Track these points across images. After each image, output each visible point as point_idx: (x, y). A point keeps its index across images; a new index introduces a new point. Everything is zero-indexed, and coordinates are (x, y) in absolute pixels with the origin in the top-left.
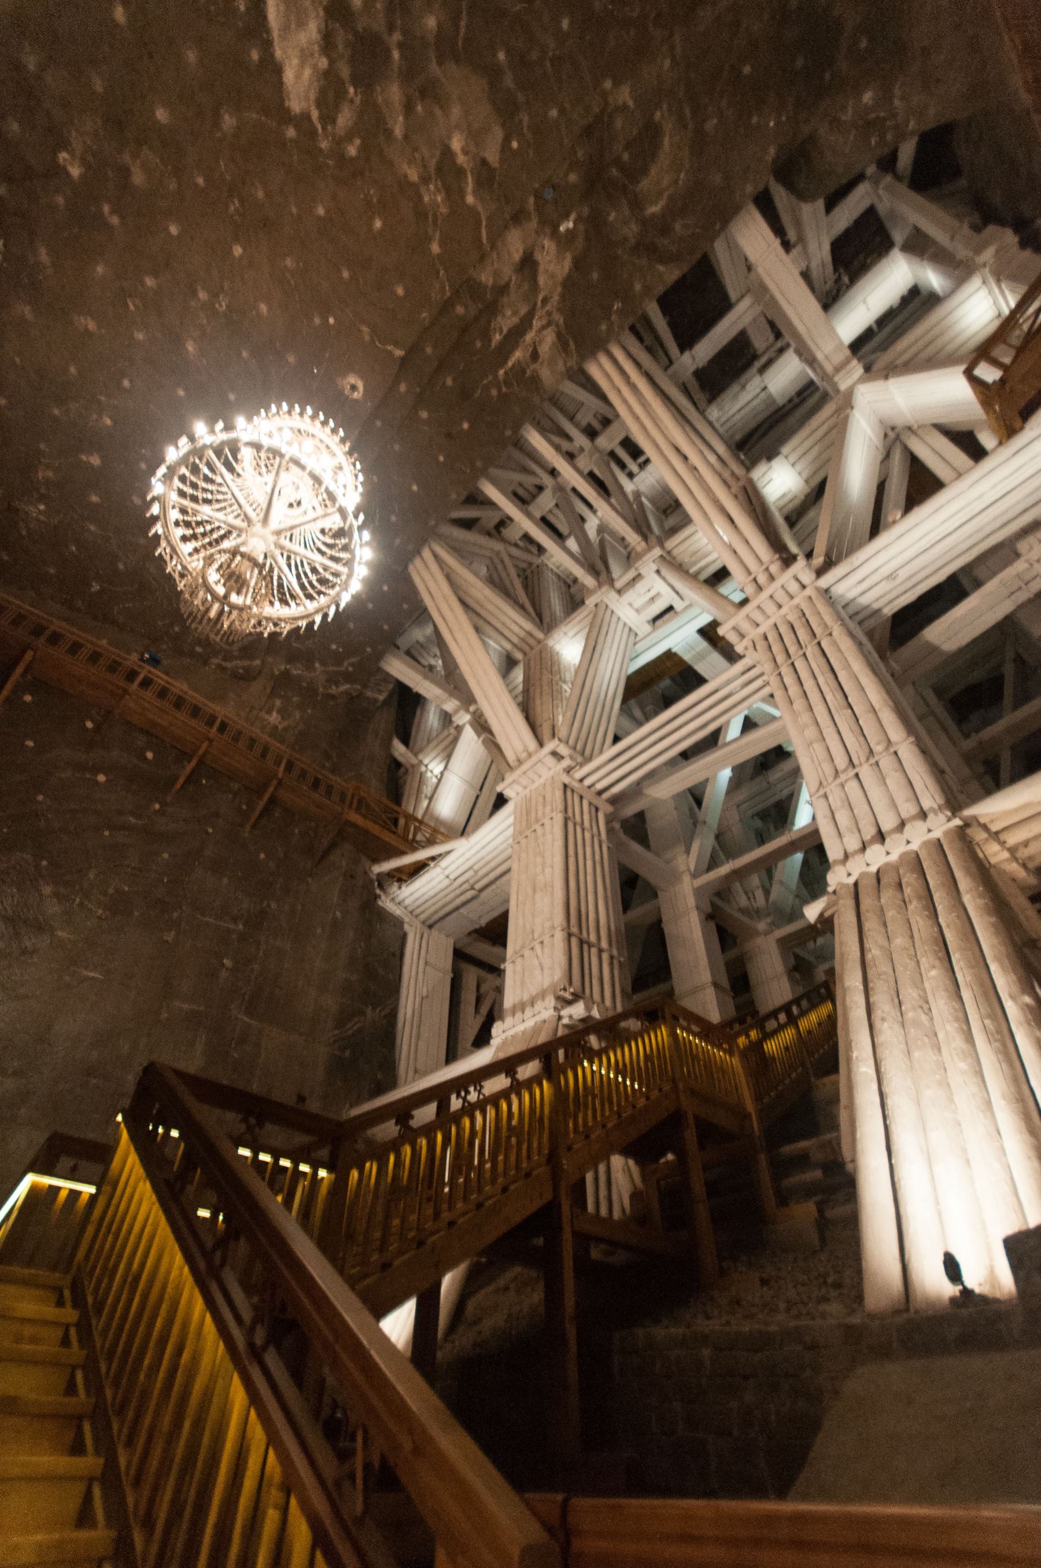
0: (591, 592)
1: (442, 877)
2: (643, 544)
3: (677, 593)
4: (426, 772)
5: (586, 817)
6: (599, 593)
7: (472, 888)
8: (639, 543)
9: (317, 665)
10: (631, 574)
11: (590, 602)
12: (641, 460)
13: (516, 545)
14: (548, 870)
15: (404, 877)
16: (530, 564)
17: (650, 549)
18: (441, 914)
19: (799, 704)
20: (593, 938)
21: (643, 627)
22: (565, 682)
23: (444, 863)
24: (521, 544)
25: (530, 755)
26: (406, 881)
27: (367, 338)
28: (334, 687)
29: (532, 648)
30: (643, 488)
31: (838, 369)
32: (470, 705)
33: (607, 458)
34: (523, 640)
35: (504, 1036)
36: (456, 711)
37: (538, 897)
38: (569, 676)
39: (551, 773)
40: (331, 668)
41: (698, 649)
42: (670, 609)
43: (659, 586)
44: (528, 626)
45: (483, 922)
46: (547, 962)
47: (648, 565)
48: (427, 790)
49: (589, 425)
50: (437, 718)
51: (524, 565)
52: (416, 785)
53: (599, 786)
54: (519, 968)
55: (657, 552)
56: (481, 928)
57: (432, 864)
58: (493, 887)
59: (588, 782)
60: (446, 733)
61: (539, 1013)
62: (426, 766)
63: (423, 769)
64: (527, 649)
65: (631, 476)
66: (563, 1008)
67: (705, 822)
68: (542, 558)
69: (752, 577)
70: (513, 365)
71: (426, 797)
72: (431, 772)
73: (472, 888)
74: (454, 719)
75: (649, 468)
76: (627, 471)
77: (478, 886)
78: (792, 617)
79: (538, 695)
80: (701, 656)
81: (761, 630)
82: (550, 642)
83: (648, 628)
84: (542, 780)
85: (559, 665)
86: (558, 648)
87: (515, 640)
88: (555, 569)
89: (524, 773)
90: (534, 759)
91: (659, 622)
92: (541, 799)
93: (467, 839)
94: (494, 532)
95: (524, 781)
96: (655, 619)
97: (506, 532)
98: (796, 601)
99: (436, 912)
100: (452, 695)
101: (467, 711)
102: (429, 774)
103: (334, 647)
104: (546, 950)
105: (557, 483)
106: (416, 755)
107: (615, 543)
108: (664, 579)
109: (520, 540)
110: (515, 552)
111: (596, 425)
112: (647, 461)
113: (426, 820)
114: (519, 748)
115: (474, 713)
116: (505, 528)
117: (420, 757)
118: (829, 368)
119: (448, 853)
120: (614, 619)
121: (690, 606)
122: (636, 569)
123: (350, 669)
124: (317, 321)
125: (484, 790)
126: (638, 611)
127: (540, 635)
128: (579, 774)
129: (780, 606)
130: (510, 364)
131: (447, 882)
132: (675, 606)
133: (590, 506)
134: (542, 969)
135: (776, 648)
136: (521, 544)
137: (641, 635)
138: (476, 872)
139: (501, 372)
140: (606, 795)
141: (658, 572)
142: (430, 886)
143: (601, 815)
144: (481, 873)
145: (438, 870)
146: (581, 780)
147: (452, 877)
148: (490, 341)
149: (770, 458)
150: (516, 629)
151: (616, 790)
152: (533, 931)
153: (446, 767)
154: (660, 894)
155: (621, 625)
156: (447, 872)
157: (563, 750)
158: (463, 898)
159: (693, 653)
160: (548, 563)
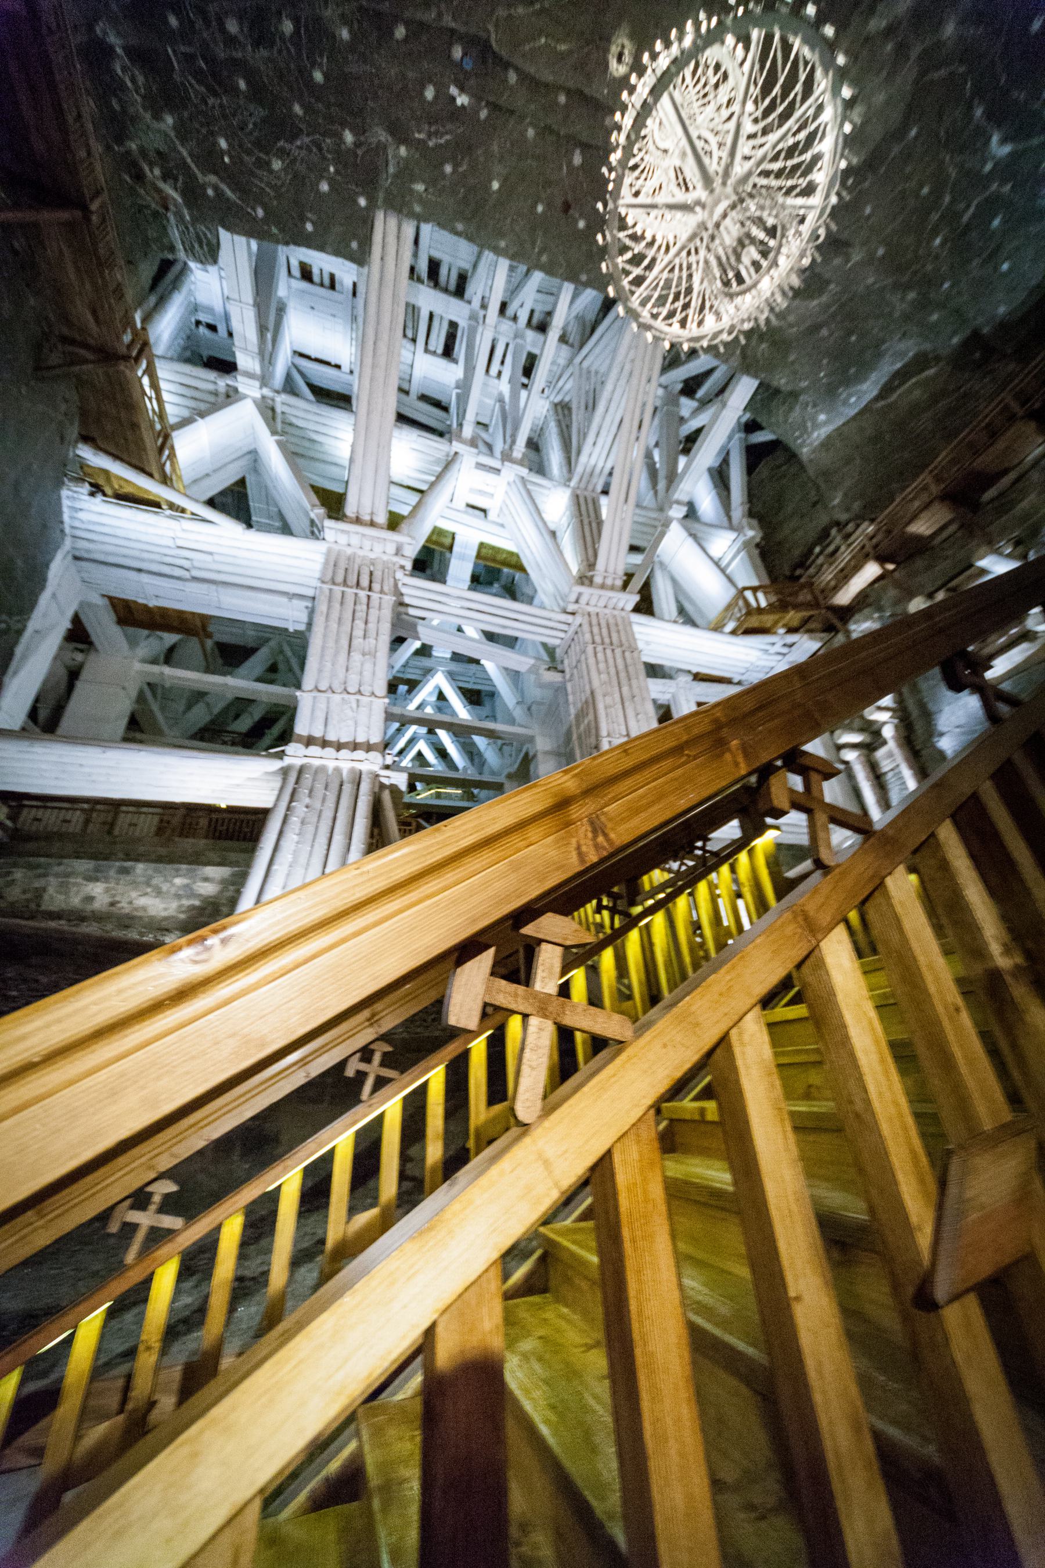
7: (187, 570)
9: (170, 120)
10: (496, 463)
11: (457, 446)
14: (372, 641)
15: (108, 491)
17: (520, 463)
18: (111, 559)
19: (604, 677)
25: (372, 524)
26: (105, 495)
28: (157, 172)
31: (678, 502)
35: (305, 761)
37: (356, 656)
39: (385, 558)
40: (185, 153)
42: (484, 511)
53: (407, 600)
54: (322, 706)
55: (524, 472)
57: (168, 512)
58: (213, 587)
73: (187, 570)
77: (195, 573)
78: (612, 621)
80: (462, 557)
81: (590, 609)
83: (462, 506)
84: (372, 556)
89: (363, 535)
91: (471, 510)
95: (355, 540)
96: (469, 506)
98: (616, 612)
99: (107, 554)
101: (261, 388)
103: (223, 144)
121: (502, 526)
123: (210, 192)
131: (171, 543)
135: (596, 630)
137: (454, 505)
144: (215, 567)
145: (173, 523)
147: (180, 543)
151: (412, 611)
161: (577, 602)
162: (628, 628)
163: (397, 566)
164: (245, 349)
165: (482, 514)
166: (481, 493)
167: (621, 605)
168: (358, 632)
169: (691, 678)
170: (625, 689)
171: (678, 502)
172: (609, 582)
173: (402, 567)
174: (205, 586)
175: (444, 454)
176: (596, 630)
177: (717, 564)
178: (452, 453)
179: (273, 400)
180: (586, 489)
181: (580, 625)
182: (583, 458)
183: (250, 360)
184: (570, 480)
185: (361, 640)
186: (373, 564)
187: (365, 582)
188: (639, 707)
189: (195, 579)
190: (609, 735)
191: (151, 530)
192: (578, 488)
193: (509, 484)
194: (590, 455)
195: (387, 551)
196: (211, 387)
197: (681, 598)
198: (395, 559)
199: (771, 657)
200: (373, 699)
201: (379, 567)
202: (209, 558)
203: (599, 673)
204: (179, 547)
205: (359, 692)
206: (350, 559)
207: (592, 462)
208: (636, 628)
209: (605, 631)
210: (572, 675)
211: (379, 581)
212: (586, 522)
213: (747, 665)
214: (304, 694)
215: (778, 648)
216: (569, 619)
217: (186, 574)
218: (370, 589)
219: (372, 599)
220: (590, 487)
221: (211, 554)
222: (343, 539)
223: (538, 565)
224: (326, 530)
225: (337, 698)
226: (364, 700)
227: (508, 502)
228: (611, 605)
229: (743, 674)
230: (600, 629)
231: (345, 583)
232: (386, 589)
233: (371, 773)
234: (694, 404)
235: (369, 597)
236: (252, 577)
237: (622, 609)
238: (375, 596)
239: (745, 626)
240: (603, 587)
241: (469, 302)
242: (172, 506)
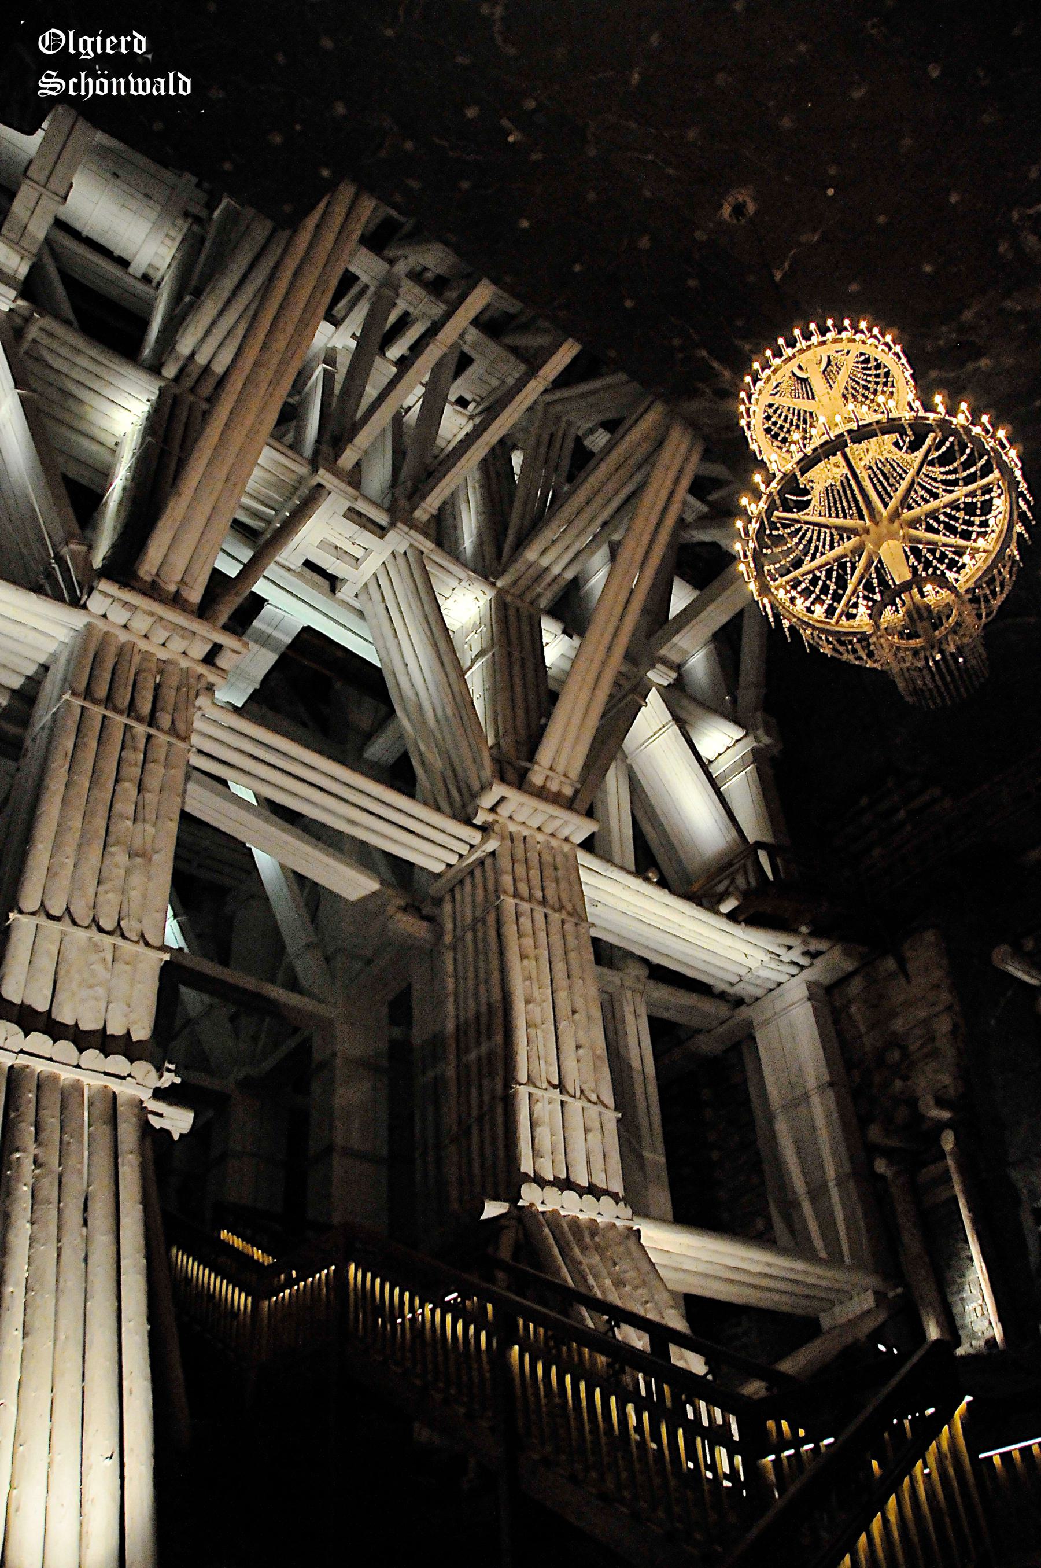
2: (425, 517)
6: (343, 486)
8: (425, 510)
10: (382, 519)
11: (324, 477)
17: (423, 530)
25: (176, 601)
27: (804, 239)
29: (192, 390)
31: (664, 661)
39: (184, 663)
41: (277, 634)
42: (333, 582)
47: (399, 540)
55: (427, 545)
69: (550, 773)
70: (714, 368)
78: (547, 858)
81: (512, 828)
83: (297, 563)
84: (162, 654)
91: (307, 572)
95: (141, 624)
96: (308, 564)
118: (663, 652)
121: (361, 614)
124: (832, 171)
129: (539, 829)
130: (715, 364)
139: (704, 353)
148: (744, 338)
149: (564, 632)
159: (269, 630)
161: (493, 809)
162: (573, 876)
165: (326, 584)
167: (565, 832)
168: (125, 807)
169: (647, 972)
170: (562, 995)
171: (664, 661)
172: (554, 787)
175: (295, 477)
176: (520, 869)
177: (704, 765)
180: (520, 597)
181: (493, 853)
182: (531, 554)
184: (497, 577)
185: (129, 823)
186: (161, 672)
187: (146, 708)
188: (581, 1033)
190: (530, 1081)
192: (507, 592)
193: (393, 553)
194: (544, 552)
195: (190, 653)
197: (640, 815)
198: (202, 669)
199: (782, 968)
200: (141, 948)
201: (174, 681)
203: (523, 956)
205: (119, 931)
206: (123, 652)
207: (545, 562)
208: (584, 876)
209: (535, 873)
210: (458, 940)
211: (170, 708)
212: (516, 655)
213: (743, 972)
215: (795, 955)
216: (476, 837)
218: (152, 721)
219: (154, 741)
220: (529, 596)
222: (118, 616)
223: (420, 707)
224: (95, 594)
227: (383, 581)
228: (549, 830)
229: (732, 984)
230: (528, 869)
231: (109, 701)
234: (705, 509)
235: (149, 737)
237: (566, 840)
238: (162, 738)
239: (752, 911)
240: (541, 794)
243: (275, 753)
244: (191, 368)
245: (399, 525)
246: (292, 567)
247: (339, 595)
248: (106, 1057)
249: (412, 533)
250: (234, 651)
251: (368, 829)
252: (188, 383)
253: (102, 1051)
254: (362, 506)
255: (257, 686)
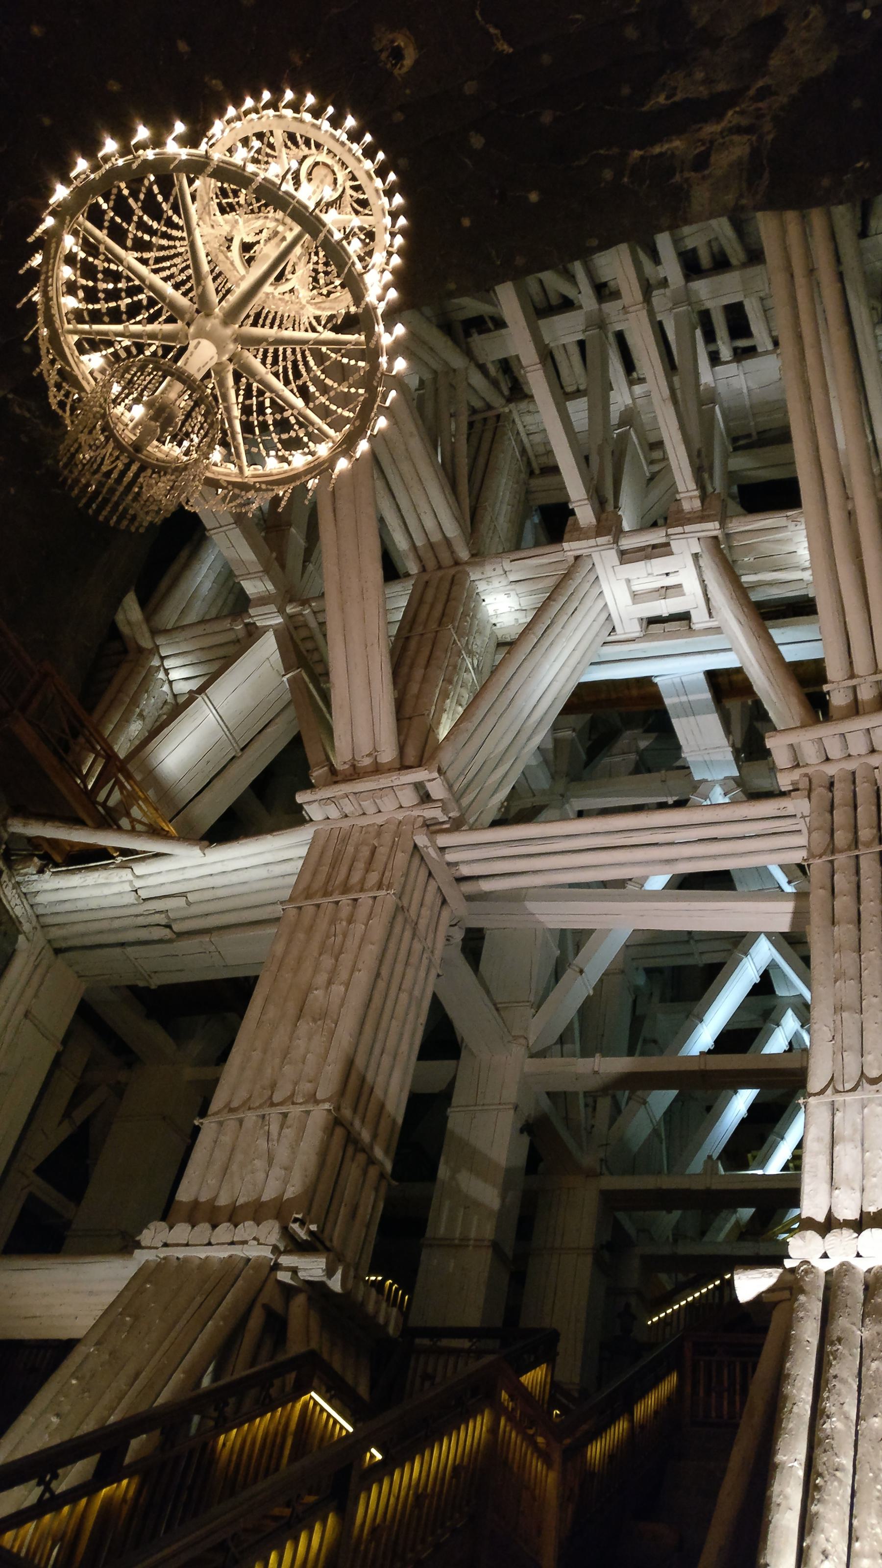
0: (582, 534)
1: (128, 888)
2: (697, 504)
3: (707, 600)
4: (158, 669)
5: (425, 912)
6: (592, 542)
7: (168, 926)
8: (691, 498)
11: (571, 548)
12: (742, 343)
13: (482, 368)
16: (489, 407)
17: (702, 517)
20: (366, 1136)
21: (630, 627)
22: (470, 653)
23: (140, 869)
24: (492, 370)
25: (377, 769)
30: (722, 389)
32: (291, 601)
33: (695, 318)
34: (431, 545)
36: (263, 601)
37: (304, 1027)
38: (479, 643)
39: (400, 816)
41: (692, 698)
42: (684, 617)
43: (688, 578)
44: (452, 530)
45: (155, 982)
46: (282, 1153)
48: (150, 704)
49: (694, 250)
50: (212, 577)
51: (478, 404)
52: (134, 687)
53: (465, 871)
54: (226, 1139)
55: (712, 528)
56: (147, 989)
57: (119, 859)
58: (206, 939)
59: (450, 857)
60: (227, 624)
61: (245, 1242)
62: (162, 658)
63: (156, 662)
64: (431, 564)
65: (715, 359)
66: (287, 1252)
67: (581, 972)
68: (512, 406)
71: (141, 716)
72: (167, 674)
74: (252, 611)
75: (750, 364)
76: (712, 348)
77: (177, 927)
79: (422, 660)
80: (691, 710)
82: (474, 575)
83: (635, 629)
84: (380, 820)
85: (474, 617)
86: (481, 587)
87: (420, 542)
88: (523, 434)
90: (384, 781)
91: (656, 628)
92: (365, 852)
93: (202, 849)
94: (459, 330)
97: (478, 341)
100: (267, 571)
101: (281, 611)
102: (161, 675)
104: (286, 1131)
105: (600, 310)
106: (155, 632)
107: (640, 451)
108: (698, 568)
109: (493, 362)
110: (477, 379)
111: (705, 259)
112: (750, 352)
113: (130, 767)
114: (364, 745)
115: (291, 617)
116: (480, 332)
117: (160, 641)
119: (157, 855)
120: (595, 592)
121: (717, 630)
122: (667, 535)
125: (249, 751)
126: (636, 597)
127: (464, 554)
128: (443, 840)
131: (131, 899)
132: (694, 618)
133: (629, 366)
134: (270, 1164)
136: (492, 370)
138: (189, 904)
140: (468, 888)
141: (696, 556)
142: (97, 892)
143: (445, 915)
144: (194, 910)
145: (126, 874)
146: (443, 849)
147: (143, 894)
150: (429, 523)
151: (486, 886)
152: (273, 1086)
153: (202, 690)
154: (464, 1053)
155: (600, 604)
156: (138, 884)
157: (437, 790)
158: (143, 935)
159: (684, 699)
160: (517, 420)
163: (420, 822)
164: (248, 575)
166: (665, 591)
173: (431, 827)
174: (196, 941)
178: (571, 560)
179: (302, 614)
183: (259, 584)
189: (181, 935)
191: (107, 891)
196: (231, 636)
198: (416, 812)
202: (181, 902)
204: (144, 900)
214: (205, 1121)
217: (166, 933)
221: (183, 895)
222: (333, 812)
225: (251, 1118)
226: (295, 1111)
232: (385, 882)
233: (259, 1264)
236: (222, 912)
238: (365, 898)
241: (580, 307)
242: (125, 852)
243: (534, 842)
244: (421, 553)
245: (671, 531)
246: (637, 635)
247: (694, 627)
248: (236, 1226)
249: (688, 528)
250: (429, 781)
251: (690, 859)
252: (431, 564)
253: (254, 1220)
254: (627, 543)
255: (731, 749)
